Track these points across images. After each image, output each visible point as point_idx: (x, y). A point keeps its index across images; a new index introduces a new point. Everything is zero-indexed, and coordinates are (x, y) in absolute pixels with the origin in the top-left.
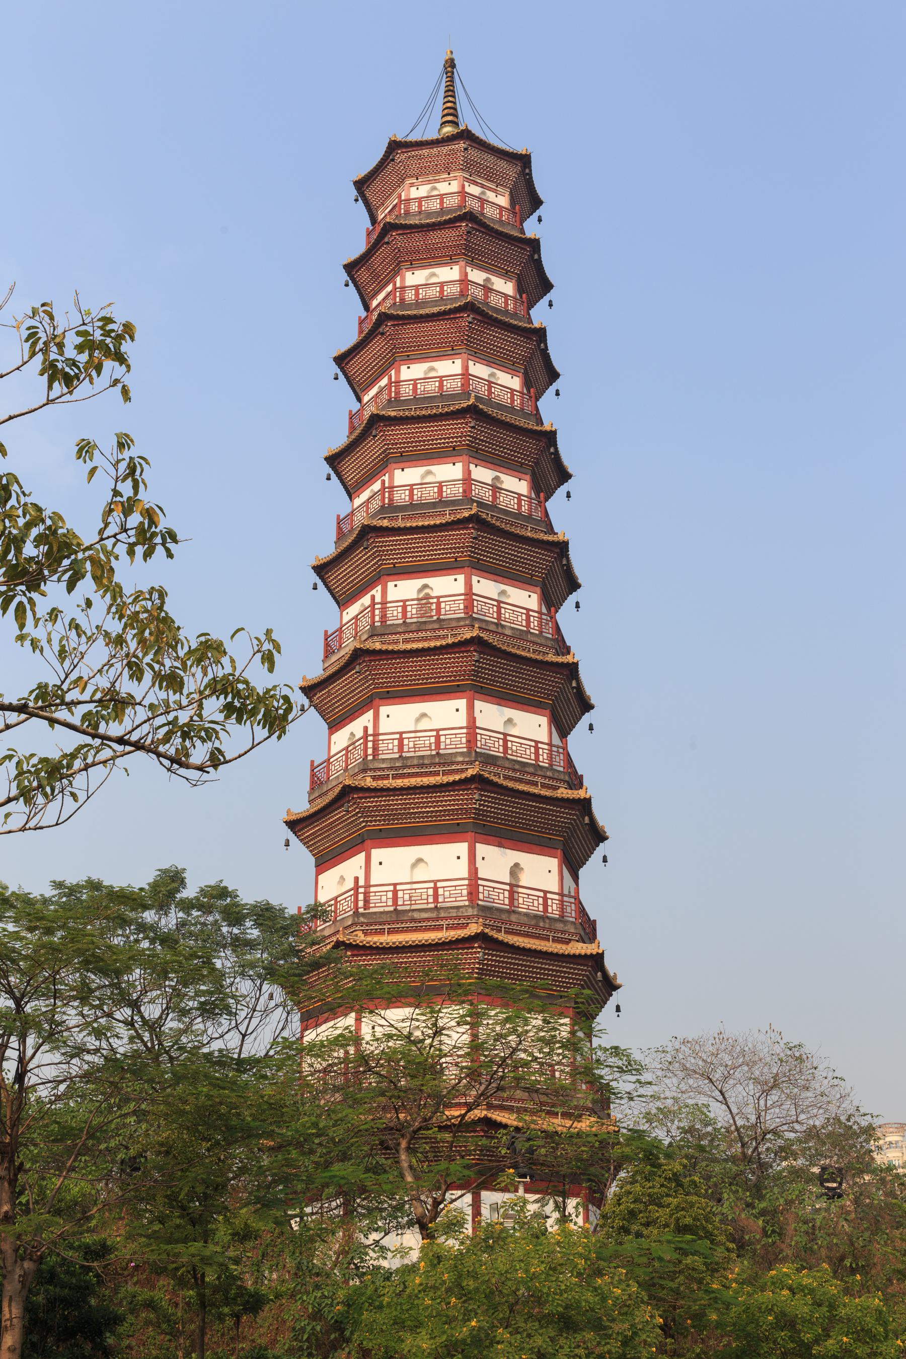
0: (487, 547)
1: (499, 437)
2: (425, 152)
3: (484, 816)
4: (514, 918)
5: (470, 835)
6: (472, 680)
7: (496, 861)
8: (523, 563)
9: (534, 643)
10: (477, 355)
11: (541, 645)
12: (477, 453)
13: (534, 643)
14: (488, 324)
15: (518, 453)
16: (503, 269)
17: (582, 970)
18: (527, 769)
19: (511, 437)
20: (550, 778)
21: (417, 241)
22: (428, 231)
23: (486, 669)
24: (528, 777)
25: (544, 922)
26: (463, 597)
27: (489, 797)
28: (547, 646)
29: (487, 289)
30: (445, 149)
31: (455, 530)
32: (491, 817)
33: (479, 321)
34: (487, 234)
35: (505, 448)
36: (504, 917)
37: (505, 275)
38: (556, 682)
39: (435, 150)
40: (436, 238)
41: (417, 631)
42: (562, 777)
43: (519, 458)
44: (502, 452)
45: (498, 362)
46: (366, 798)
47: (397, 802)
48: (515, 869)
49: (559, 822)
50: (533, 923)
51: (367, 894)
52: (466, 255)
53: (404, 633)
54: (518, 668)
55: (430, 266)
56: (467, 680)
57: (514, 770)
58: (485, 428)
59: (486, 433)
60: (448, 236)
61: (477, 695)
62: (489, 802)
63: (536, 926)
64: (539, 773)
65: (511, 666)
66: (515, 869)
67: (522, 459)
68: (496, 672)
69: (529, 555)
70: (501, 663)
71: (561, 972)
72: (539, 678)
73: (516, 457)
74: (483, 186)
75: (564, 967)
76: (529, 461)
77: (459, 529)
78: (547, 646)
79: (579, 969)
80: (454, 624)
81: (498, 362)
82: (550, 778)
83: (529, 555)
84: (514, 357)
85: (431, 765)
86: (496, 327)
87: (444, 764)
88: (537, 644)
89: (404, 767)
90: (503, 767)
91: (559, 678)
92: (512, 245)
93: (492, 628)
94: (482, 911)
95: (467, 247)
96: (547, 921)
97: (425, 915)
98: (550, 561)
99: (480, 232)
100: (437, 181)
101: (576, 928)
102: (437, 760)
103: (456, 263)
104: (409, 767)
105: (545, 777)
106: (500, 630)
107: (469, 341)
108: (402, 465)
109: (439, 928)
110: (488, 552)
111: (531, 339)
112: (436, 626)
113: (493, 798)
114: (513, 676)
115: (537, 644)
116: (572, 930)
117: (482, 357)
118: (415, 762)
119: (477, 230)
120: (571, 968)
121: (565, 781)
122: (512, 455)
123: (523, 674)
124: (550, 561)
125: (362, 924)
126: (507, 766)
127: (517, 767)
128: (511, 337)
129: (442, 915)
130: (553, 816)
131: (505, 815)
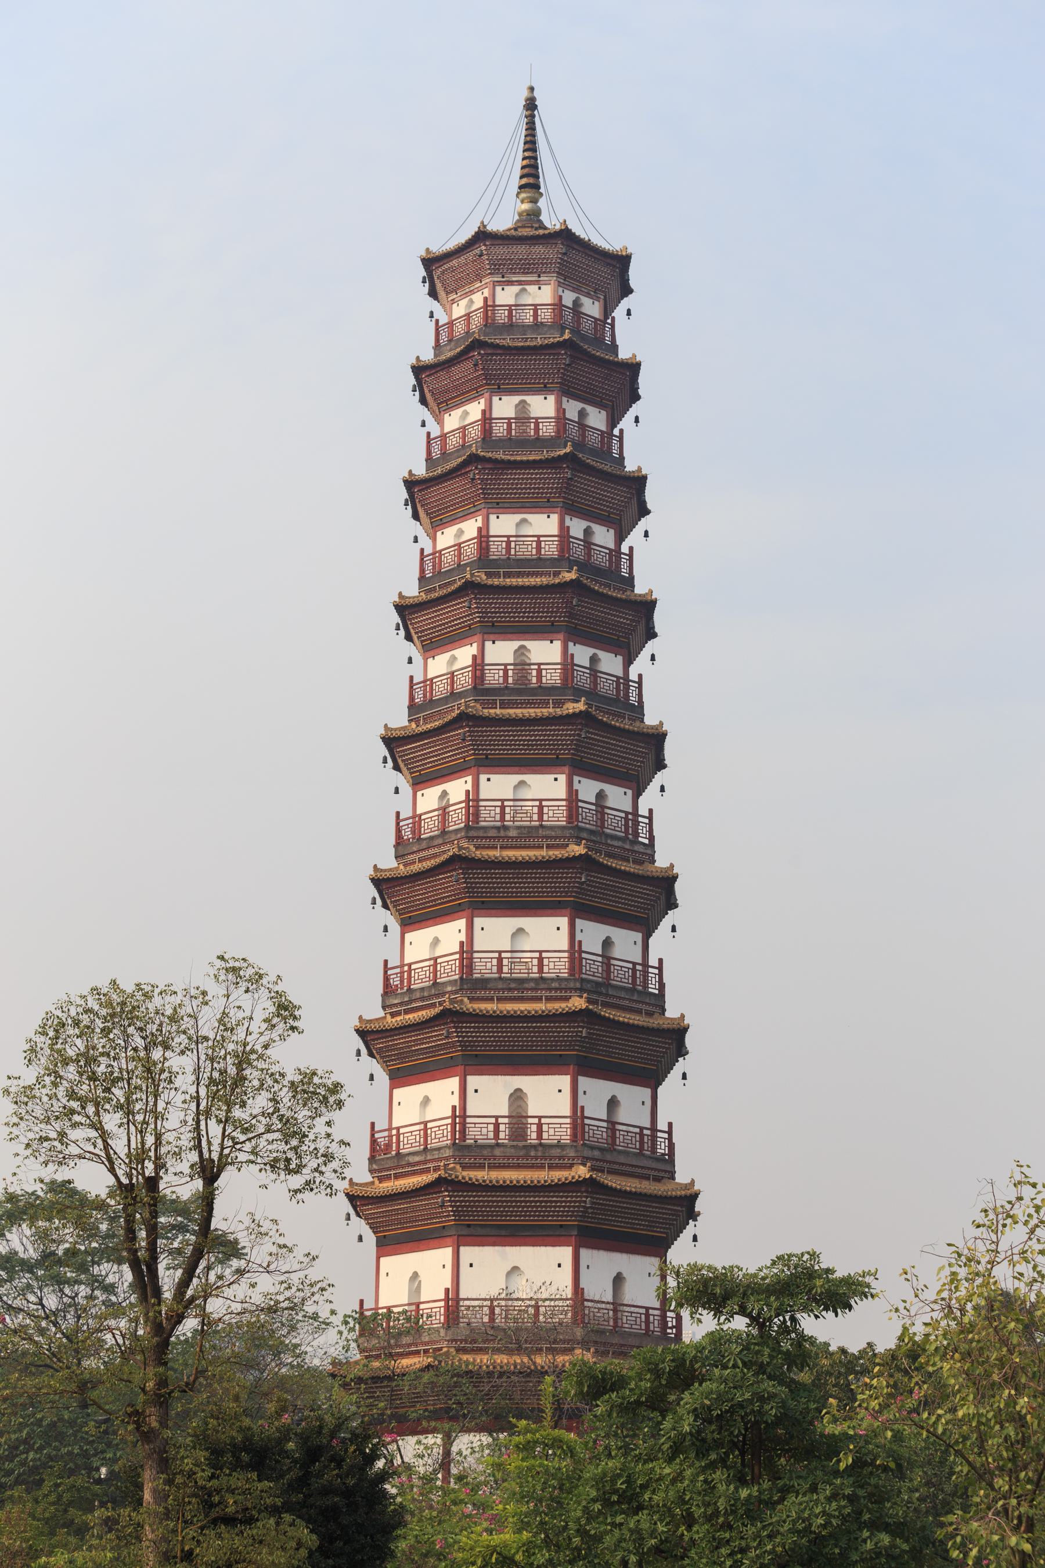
0: (491, 740)
1: (513, 603)
2: (455, 263)
3: (472, 1046)
4: (497, 1152)
5: (460, 1069)
6: (469, 897)
7: (490, 1095)
8: (541, 745)
9: (547, 837)
10: (501, 505)
11: (556, 838)
12: (495, 629)
13: (547, 837)
14: (503, 469)
15: (543, 612)
16: (539, 383)
17: (577, 1197)
18: (526, 986)
19: (528, 599)
20: (556, 990)
22: (450, 367)
23: (481, 883)
24: (530, 994)
25: (537, 1150)
26: (436, 813)
27: (470, 1027)
28: (565, 837)
29: (522, 416)
30: (470, 256)
31: (452, 731)
32: (481, 1046)
33: (490, 469)
34: (506, 355)
35: (524, 613)
36: (485, 1152)
37: (543, 389)
38: (571, 878)
39: (462, 259)
41: (428, 848)
42: (572, 985)
43: (546, 617)
44: (523, 617)
45: (528, 505)
46: (377, 1039)
47: (399, 1041)
48: (517, 1097)
49: (563, 1037)
50: (522, 1153)
51: (464, 1124)
52: (489, 385)
54: (518, 874)
55: (462, 404)
56: (465, 898)
57: (510, 990)
58: (493, 599)
59: (496, 603)
61: (476, 912)
62: (472, 1032)
63: (526, 1156)
64: (542, 986)
65: (509, 874)
66: (517, 1097)
67: (550, 617)
68: (494, 883)
69: (545, 735)
70: (496, 874)
71: (551, 1202)
72: (548, 878)
73: (541, 617)
74: (520, 283)
75: (553, 1197)
76: (560, 617)
77: (457, 729)
78: (565, 837)
79: (572, 1197)
81: (528, 505)
82: (556, 990)
83: (545, 735)
84: (546, 493)
85: (430, 997)
86: (512, 469)
88: (551, 838)
89: (411, 1001)
90: (495, 990)
91: (572, 873)
92: (541, 355)
93: (492, 833)
94: (459, 1150)
95: (487, 377)
96: (540, 1149)
97: (417, 1159)
98: (574, 735)
99: (496, 355)
101: (577, 1151)
104: (415, 1000)
105: (550, 990)
106: (502, 833)
107: (485, 494)
109: (427, 1171)
110: (494, 745)
111: (561, 468)
112: (440, 841)
113: (474, 1027)
114: (515, 883)
115: (551, 838)
116: (572, 1154)
117: (506, 505)
118: (418, 995)
119: (492, 355)
120: (562, 1197)
121: (576, 989)
122: (537, 617)
123: (526, 878)
124: (574, 735)
126: (500, 986)
127: (513, 985)
128: (534, 474)
129: (429, 1158)
130: (554, 1032)
131: (497, 1042)
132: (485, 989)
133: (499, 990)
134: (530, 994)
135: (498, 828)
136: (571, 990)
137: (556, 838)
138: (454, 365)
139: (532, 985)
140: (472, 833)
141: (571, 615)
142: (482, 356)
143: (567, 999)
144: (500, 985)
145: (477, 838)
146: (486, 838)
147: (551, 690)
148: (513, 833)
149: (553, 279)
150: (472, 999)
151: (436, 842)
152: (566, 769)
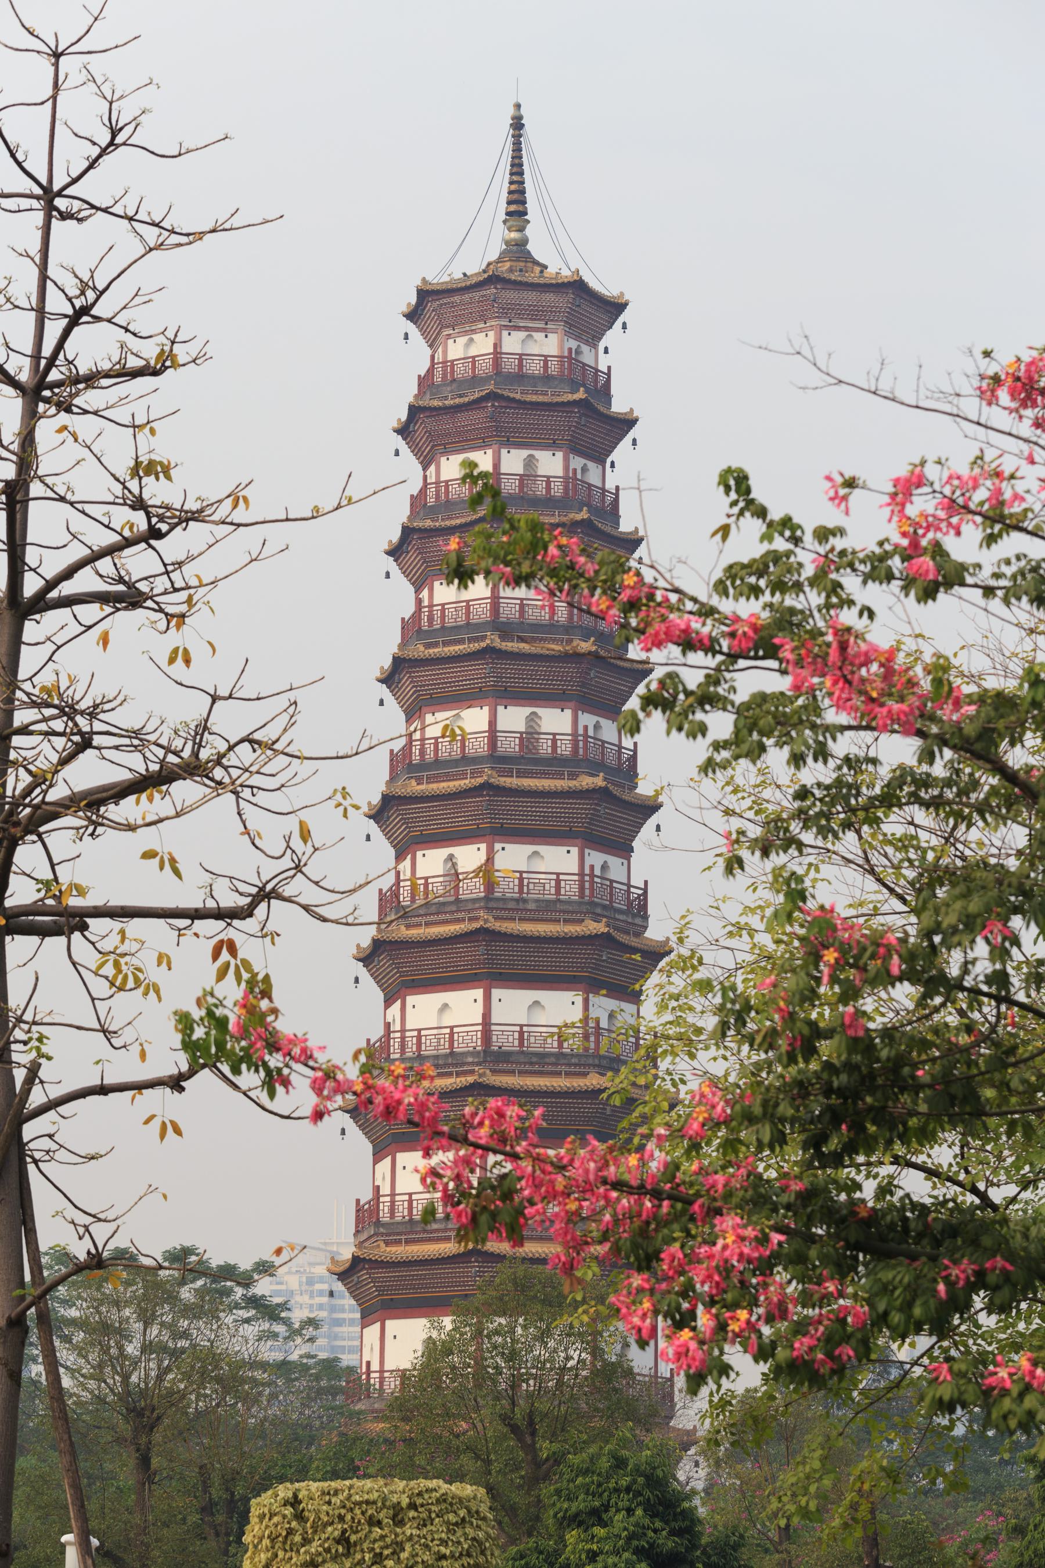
2: (457, 299)
9: (564, 912)
11: (573, 912)
13: (564, 912)
18: (547, 1060)
20: (575, 1065)
21: (446, 424)
24: (550, 1068)
30: (477, 295)
37: (552, 445)
39: (466, 297)
40: (463, 419)
41: (437, 914)
53: (426, 915)
57: (531, 1064)
60: (476, 418)
64: (562, 1061)
74: (527, 329)
78: (581, 913)
80: (470, 906)
82: (575, 1065)
85: (446, 1065)
87: (456, 1065)
88: (568, 912)
93: (511, 905)
100: (474, 332)
102: (450, 1061)
103: (489, 446)
105: (569, 1065)
106: (521, 906)
108: (432, 708)
112: (454, 908)
115: (568, 912)
119: (506, 407)
121: (594, 1066)
125: (382, 1234)
127: (534, 1060)
132: (508, 1062)
133: (520, 1063)
134: (550, 1068)
135: (517, 900)
136: (589, 1065)
137: (573, 912)
138: (461, 411)
139: (553, 1060)
140: (492, 904)
141: (583, 685)
142: (496, 408)
143: (585, 1075)
144: (522, 1059)
145: (497, 909)
146: (505, 909)
147: (563, 761)
148: (531, 906)
149: (561, 327)
150: (494, 1072)
151: (448, 909)
152: (578, 841)
